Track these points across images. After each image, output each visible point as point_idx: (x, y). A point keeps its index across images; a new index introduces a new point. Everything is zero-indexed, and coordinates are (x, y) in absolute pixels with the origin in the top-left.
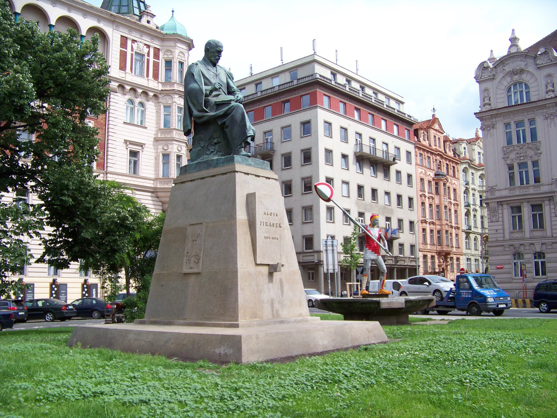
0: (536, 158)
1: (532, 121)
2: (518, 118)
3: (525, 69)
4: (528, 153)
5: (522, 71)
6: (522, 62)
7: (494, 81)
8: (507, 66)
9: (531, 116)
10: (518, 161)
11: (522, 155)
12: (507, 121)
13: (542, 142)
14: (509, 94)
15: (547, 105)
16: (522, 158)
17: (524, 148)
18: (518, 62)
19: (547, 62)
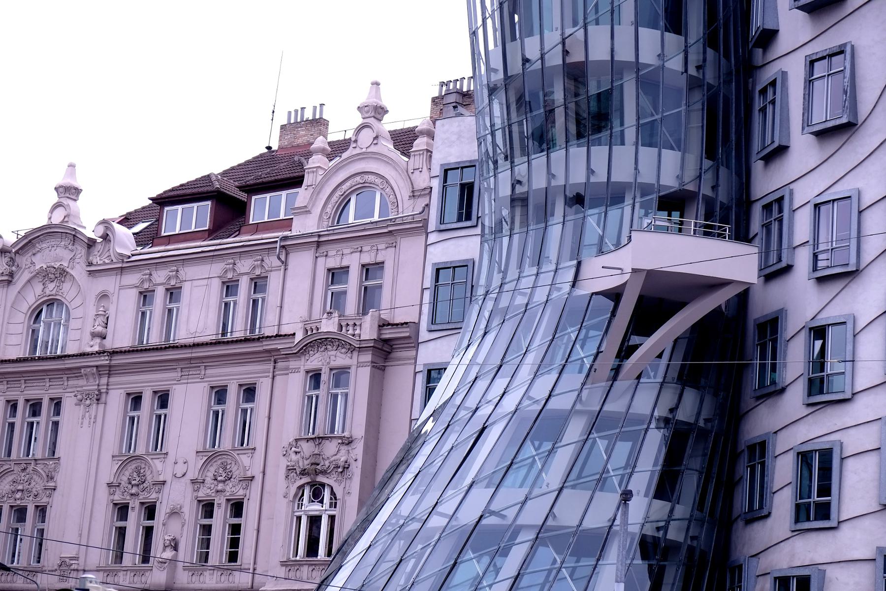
0: (43, 500)
1: (57, 404)
2: (34, 392)
3: (68, 270)
4: (33, 483)
5: (62, 274)
6: (67, 251)
7: (11, 287)
8: (39, 255)
9: (55, 392)
10: (11, 502)
11: (20, 487)
12: (12, 395)
13: (62, 461)
14: (36, 325)
15: (82, 370)
16: (18, 495)
17: (28, 471)
18: (58, 250)
19: (105, 264)
